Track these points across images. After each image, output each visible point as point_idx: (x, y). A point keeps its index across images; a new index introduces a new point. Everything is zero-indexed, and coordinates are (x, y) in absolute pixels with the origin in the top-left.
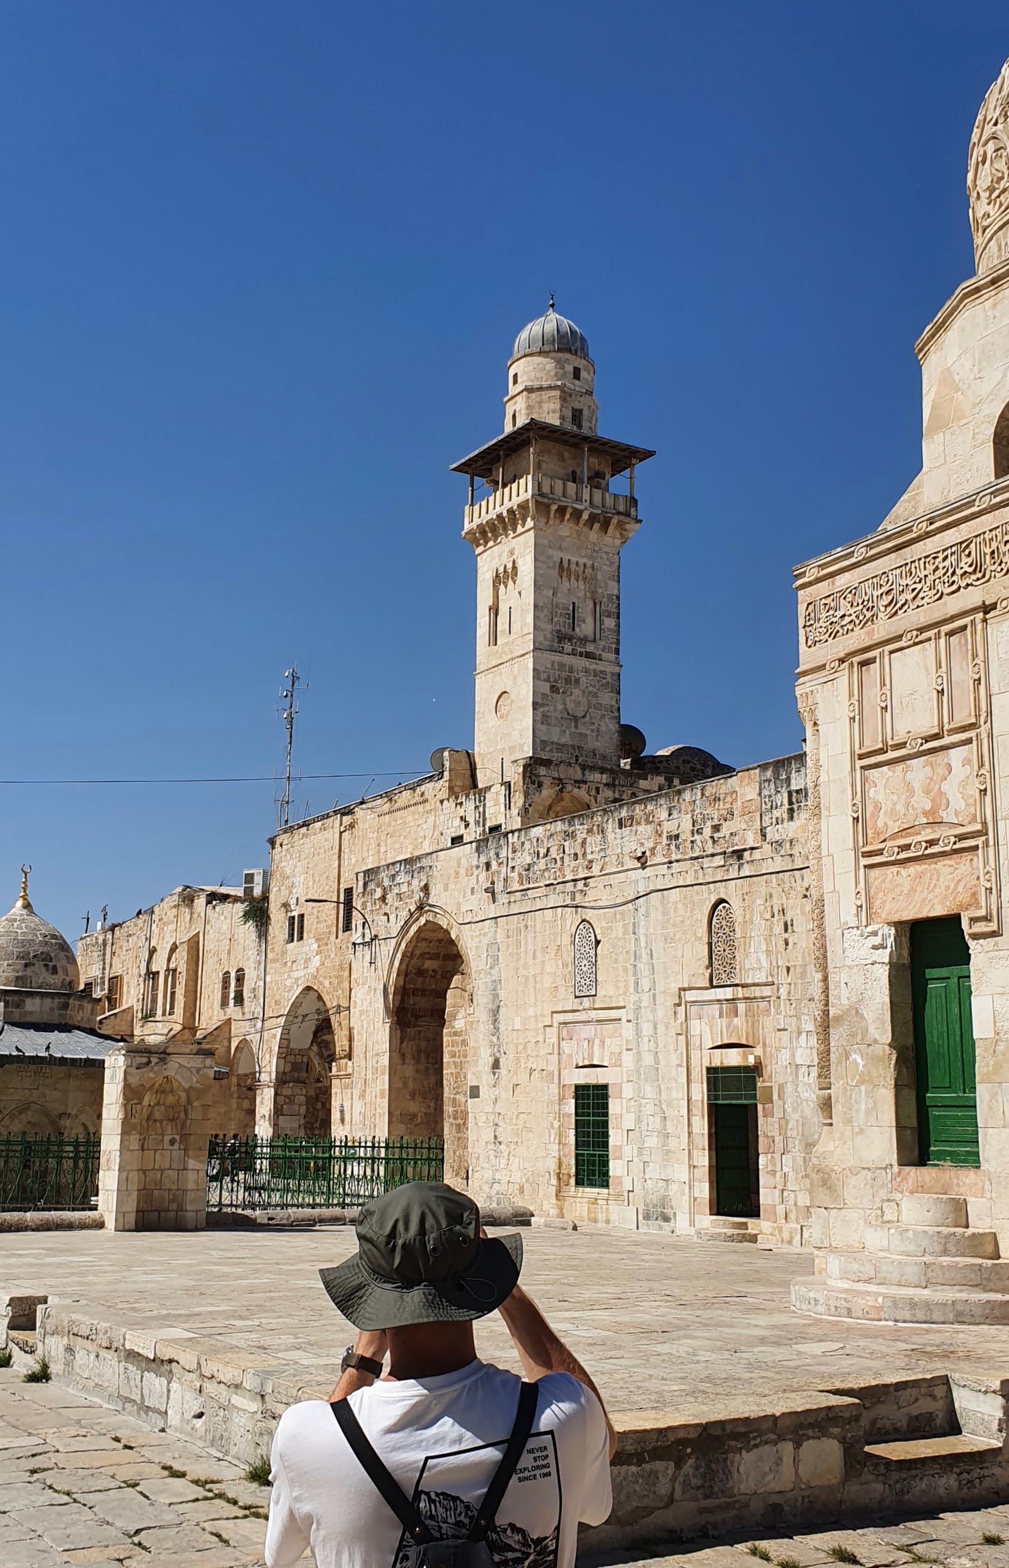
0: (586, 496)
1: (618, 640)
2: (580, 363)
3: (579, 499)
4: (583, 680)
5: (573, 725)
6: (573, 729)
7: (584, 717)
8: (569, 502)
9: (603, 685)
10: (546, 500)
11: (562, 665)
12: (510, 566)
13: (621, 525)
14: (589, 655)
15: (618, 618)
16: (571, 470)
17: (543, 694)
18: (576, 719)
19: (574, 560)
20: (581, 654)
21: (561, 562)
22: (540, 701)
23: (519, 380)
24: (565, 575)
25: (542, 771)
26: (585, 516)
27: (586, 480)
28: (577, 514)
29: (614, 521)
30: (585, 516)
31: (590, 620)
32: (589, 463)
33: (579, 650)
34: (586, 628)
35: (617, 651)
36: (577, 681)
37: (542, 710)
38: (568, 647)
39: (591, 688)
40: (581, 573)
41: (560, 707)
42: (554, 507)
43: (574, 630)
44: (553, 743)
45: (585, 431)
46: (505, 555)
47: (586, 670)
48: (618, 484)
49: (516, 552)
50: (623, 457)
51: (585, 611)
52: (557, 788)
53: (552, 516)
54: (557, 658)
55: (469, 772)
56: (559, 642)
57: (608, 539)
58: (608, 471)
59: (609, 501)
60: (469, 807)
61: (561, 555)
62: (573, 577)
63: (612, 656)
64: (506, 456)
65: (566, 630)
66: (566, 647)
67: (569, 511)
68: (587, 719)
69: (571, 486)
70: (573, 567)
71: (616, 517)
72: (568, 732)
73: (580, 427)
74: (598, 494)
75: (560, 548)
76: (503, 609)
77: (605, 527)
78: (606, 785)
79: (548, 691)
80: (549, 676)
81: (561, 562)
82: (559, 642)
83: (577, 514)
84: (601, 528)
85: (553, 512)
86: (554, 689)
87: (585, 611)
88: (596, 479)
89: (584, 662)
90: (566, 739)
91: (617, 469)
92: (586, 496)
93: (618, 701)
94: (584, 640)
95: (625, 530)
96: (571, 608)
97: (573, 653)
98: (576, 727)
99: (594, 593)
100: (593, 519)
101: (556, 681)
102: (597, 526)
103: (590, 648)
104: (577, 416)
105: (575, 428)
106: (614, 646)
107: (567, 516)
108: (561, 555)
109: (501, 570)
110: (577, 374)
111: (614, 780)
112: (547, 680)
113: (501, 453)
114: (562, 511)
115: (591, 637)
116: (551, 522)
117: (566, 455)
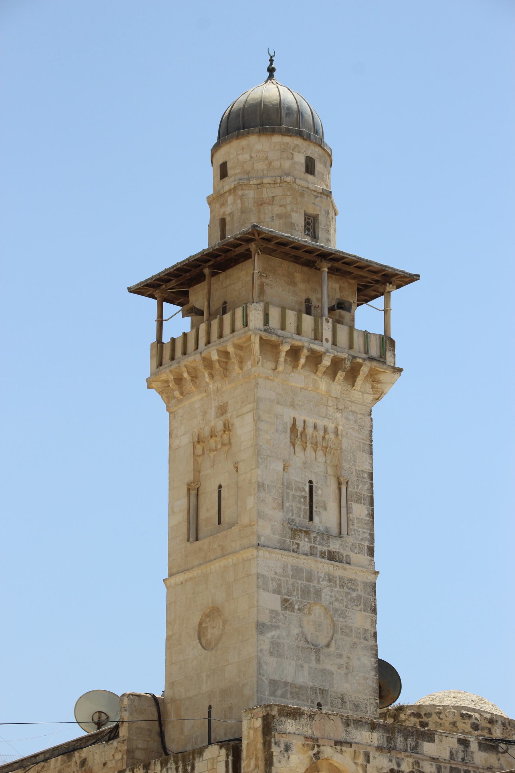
0: (327, 333)
1: (372, 535)
2: (313, 151)
3: (317, 337)
4: (326, 593)
5: (313, 658)
6: (314, 664)
7: (328, 645)
8: (305, 341)
9: (353, 600)
10: (274, 338)
11: (297, 571)
12: (220, 426)
13: (372, 376)
14: (332, 557)
15: (372, 503)
16: (304, 297)
17: (272, 611)
18: (317, 649)
19: (311, 421)
20: (322, 555)
21: (294, 425)
22: (267, 622)
23: (230, 172)
24: (298, 442)
25: (290, 725)
26: (327, 362)
27: (326, 311)
28: (315, 358)
29: (364, 370)
30: (327, 362)
31: (332, 506)
32: (329, 290)
33: (320, 548)
34: (327, 518)
35: (371, 552)
36: (318, 593)
37: (270, 635)
38: (305, 544)
39: (336, 604)
40: (320, 439)
41: (296, 631)
42: (286, 348)
43: (311, 519)
44: (286, 684)
45: (321, 244)
46: (212, 412)
47: (330, 579)
48: (367, 317)
49: (230, 409)
50: (375, 281)
51: (327, 493)
52: (311, 753)
53: (282, 359)
54: (290, 559)
55: (157, 728)
56: (293, 537)
57: (356, 394)
58: (353, 299)
59: (358, 342)
61: (293, 413)
62: (309, 445)
63: (364, 558)
64: (214, 274)
65: (302, 520)
66: (302, 543)
67: (305, 353)
68: (332, 649)
69: (308, 320)
70: (310, 431)
71: (368, 363)
72: (306, 666)
73: (315, 237)
75: (292, 405)
76: (209, 489)
77: (353, 374)
78: (379, 748)
79: (277, 606)
80: (279, 586)
81: (294, 425)
82: (293, 537)
83: (315, 358)
84: (346, 378)
85: (283, 354)
87: (327, 493)
88: (341, 308)
89: (324, 567)
90: (304, 678)
91: (365, 295)
92: (327, 333)
93: (374, 623)
95: (379, 382)
96: (307, 489)
97: (312, 553)
98: (318, 661)
99: (337, 467)
100: (336, 365)
101: (289, 593)
102: (341, 375)
103: (335, 546)
104: (311, 224)
105: (308, 239)
106: (366, 544)
107: (303, 361)
108: (293, 413)
109: (207, 432)
110: (310, 167)
111: (389, 740)
112: (277, 591)
113: (206, 271)
114: (295, 353)
115: (335, 531)
116: (281, 368)
117: (298, 277)
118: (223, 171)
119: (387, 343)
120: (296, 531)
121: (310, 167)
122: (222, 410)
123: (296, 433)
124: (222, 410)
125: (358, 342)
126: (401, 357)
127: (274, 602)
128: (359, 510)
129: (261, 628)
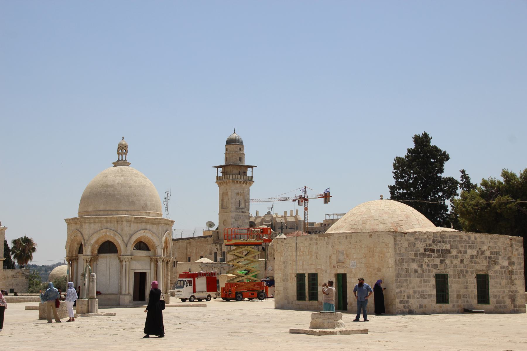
0: (242, 178)
2: (241, 146)
3: (241, 178)
4: (242, 218)
8: (239, 180)
13: (250, 183)
14: (243, 212)
28: (240, 182)
34: (242, 206)
38: (238, 211)
54: (236, 213)
57: (247, 186)
59: (247, 178)
60: (218, 246)
69: (239, 176)
74: (245, 177)
76: (225, 201)
77: (246, 183)
83: (240, 182)
86: (236, 220)
87: (242, 202)
89: (241, 214)
94: (242, 209)
100: (244, 182)
103: (243, 210)
110: (240, 149)
114: (237, 182)
118: (227, 150)
119: (252, 177)
120: (237, 209)
121: (240, 149)
122: (226, 190)
123: (237, 194)
124: (226, 190)
125: (247, 178)
126: (254, 180)
127: (234, 220)
128: (247, 204)
129: (232, 224)
